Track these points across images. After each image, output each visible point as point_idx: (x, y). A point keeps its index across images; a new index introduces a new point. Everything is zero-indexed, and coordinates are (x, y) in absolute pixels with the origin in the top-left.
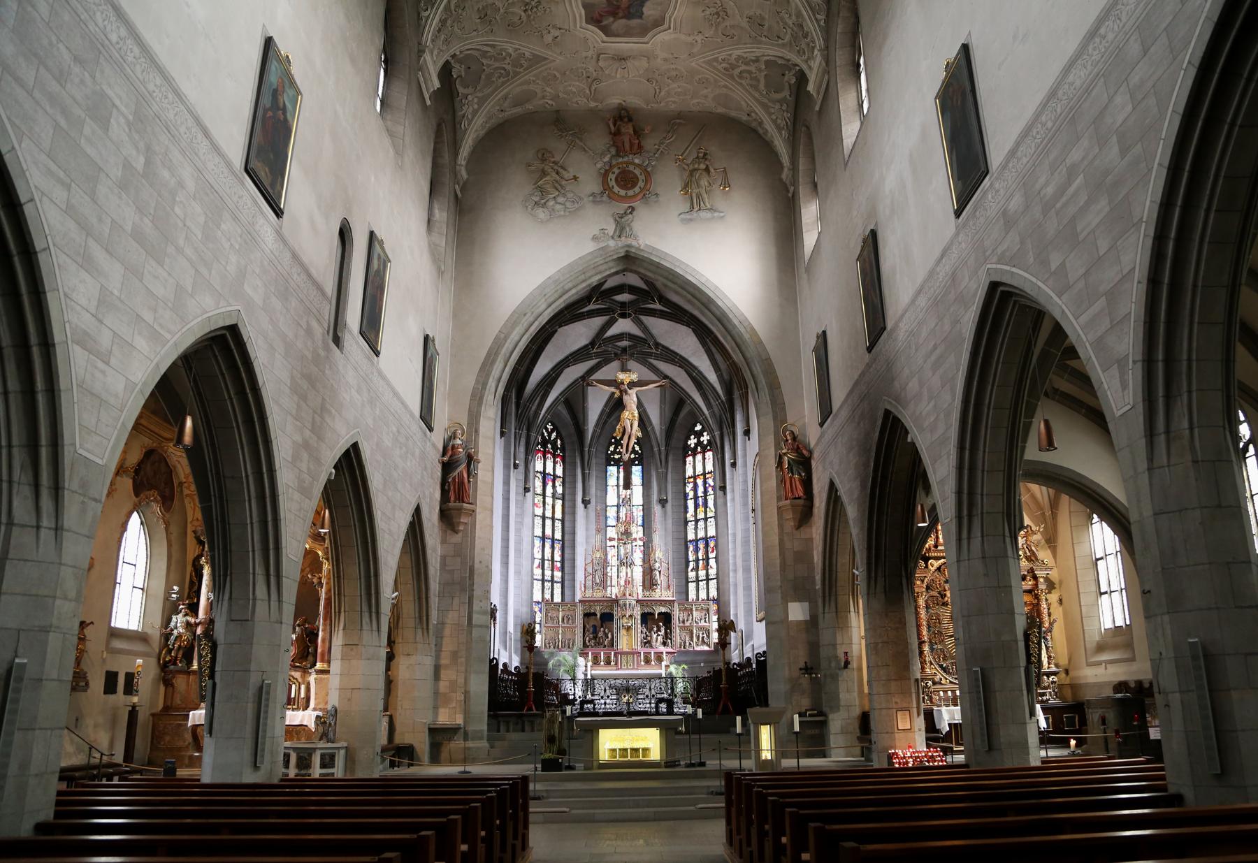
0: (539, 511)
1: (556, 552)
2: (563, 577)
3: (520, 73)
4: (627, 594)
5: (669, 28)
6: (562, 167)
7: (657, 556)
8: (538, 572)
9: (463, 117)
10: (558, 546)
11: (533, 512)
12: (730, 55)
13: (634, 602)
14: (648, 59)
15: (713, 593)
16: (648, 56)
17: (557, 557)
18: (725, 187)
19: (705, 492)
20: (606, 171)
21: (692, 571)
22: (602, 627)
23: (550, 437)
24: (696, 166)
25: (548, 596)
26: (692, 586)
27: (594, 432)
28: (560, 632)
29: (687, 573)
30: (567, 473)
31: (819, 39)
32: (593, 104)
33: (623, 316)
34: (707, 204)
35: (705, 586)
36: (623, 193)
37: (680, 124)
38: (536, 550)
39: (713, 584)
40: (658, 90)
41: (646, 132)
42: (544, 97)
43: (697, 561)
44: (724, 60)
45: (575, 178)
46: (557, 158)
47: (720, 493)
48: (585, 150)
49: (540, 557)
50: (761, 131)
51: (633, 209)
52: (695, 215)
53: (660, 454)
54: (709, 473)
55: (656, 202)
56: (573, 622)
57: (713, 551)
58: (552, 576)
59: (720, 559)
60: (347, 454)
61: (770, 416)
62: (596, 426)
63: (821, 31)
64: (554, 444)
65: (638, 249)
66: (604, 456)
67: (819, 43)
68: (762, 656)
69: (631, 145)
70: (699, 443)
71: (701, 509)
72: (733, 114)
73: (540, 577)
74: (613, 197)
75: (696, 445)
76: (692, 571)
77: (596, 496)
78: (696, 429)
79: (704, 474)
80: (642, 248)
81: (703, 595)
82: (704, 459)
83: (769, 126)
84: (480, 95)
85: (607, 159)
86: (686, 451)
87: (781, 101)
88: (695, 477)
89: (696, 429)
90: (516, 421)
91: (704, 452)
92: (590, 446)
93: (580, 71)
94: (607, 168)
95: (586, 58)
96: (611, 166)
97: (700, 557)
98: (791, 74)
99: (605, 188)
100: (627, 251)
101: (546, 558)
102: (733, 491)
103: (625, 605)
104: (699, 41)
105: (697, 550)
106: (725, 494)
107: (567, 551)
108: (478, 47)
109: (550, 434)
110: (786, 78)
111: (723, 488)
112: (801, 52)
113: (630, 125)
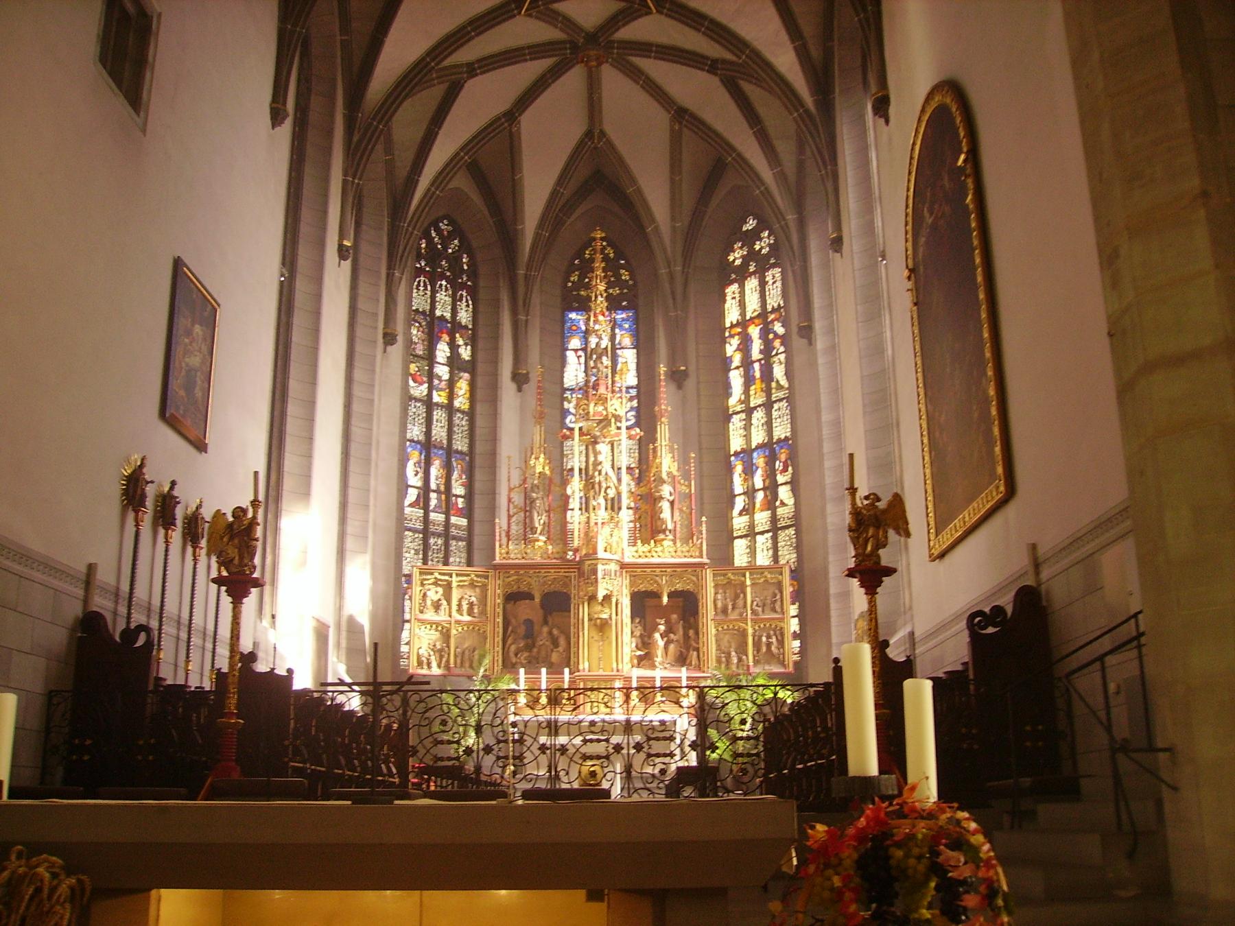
0: (420, 390)
1: (455, 475)
2: (470, 527)
7: (665, 469)
11: (406, 387)
15: (788, 556)
17: (458, 489)
19: (767, 351)
21: (740, 514)
22: (546, 622)
23: (445, 248)
26: (740, 546)
27: (537, 236)
30: (481, 321)
35: (769, 544)
38: (410, 468)
43: (750, 493)
47: (798, 343)
49: (419, 484)
53: (672, 277)
57: (785, 470)
59: (803, 481)
62: (541, 225)
64: (455, 260)
70: (752, 255)
73: (419, 526)
75: (746, 260)
76: (740, 514)
78: (744, 229)
79: (763, 315)
81: (763, 559)
82: (763, 284)
88: (743, 323)
89: (744, 229)
91: (761, 273)
92: (529, 267)
101: (433, 486)
102: (831, 331)
103: (595, 572)
105: (749, 471)
107: (479, 476)
109: (446, 242)
111: (807, 331)
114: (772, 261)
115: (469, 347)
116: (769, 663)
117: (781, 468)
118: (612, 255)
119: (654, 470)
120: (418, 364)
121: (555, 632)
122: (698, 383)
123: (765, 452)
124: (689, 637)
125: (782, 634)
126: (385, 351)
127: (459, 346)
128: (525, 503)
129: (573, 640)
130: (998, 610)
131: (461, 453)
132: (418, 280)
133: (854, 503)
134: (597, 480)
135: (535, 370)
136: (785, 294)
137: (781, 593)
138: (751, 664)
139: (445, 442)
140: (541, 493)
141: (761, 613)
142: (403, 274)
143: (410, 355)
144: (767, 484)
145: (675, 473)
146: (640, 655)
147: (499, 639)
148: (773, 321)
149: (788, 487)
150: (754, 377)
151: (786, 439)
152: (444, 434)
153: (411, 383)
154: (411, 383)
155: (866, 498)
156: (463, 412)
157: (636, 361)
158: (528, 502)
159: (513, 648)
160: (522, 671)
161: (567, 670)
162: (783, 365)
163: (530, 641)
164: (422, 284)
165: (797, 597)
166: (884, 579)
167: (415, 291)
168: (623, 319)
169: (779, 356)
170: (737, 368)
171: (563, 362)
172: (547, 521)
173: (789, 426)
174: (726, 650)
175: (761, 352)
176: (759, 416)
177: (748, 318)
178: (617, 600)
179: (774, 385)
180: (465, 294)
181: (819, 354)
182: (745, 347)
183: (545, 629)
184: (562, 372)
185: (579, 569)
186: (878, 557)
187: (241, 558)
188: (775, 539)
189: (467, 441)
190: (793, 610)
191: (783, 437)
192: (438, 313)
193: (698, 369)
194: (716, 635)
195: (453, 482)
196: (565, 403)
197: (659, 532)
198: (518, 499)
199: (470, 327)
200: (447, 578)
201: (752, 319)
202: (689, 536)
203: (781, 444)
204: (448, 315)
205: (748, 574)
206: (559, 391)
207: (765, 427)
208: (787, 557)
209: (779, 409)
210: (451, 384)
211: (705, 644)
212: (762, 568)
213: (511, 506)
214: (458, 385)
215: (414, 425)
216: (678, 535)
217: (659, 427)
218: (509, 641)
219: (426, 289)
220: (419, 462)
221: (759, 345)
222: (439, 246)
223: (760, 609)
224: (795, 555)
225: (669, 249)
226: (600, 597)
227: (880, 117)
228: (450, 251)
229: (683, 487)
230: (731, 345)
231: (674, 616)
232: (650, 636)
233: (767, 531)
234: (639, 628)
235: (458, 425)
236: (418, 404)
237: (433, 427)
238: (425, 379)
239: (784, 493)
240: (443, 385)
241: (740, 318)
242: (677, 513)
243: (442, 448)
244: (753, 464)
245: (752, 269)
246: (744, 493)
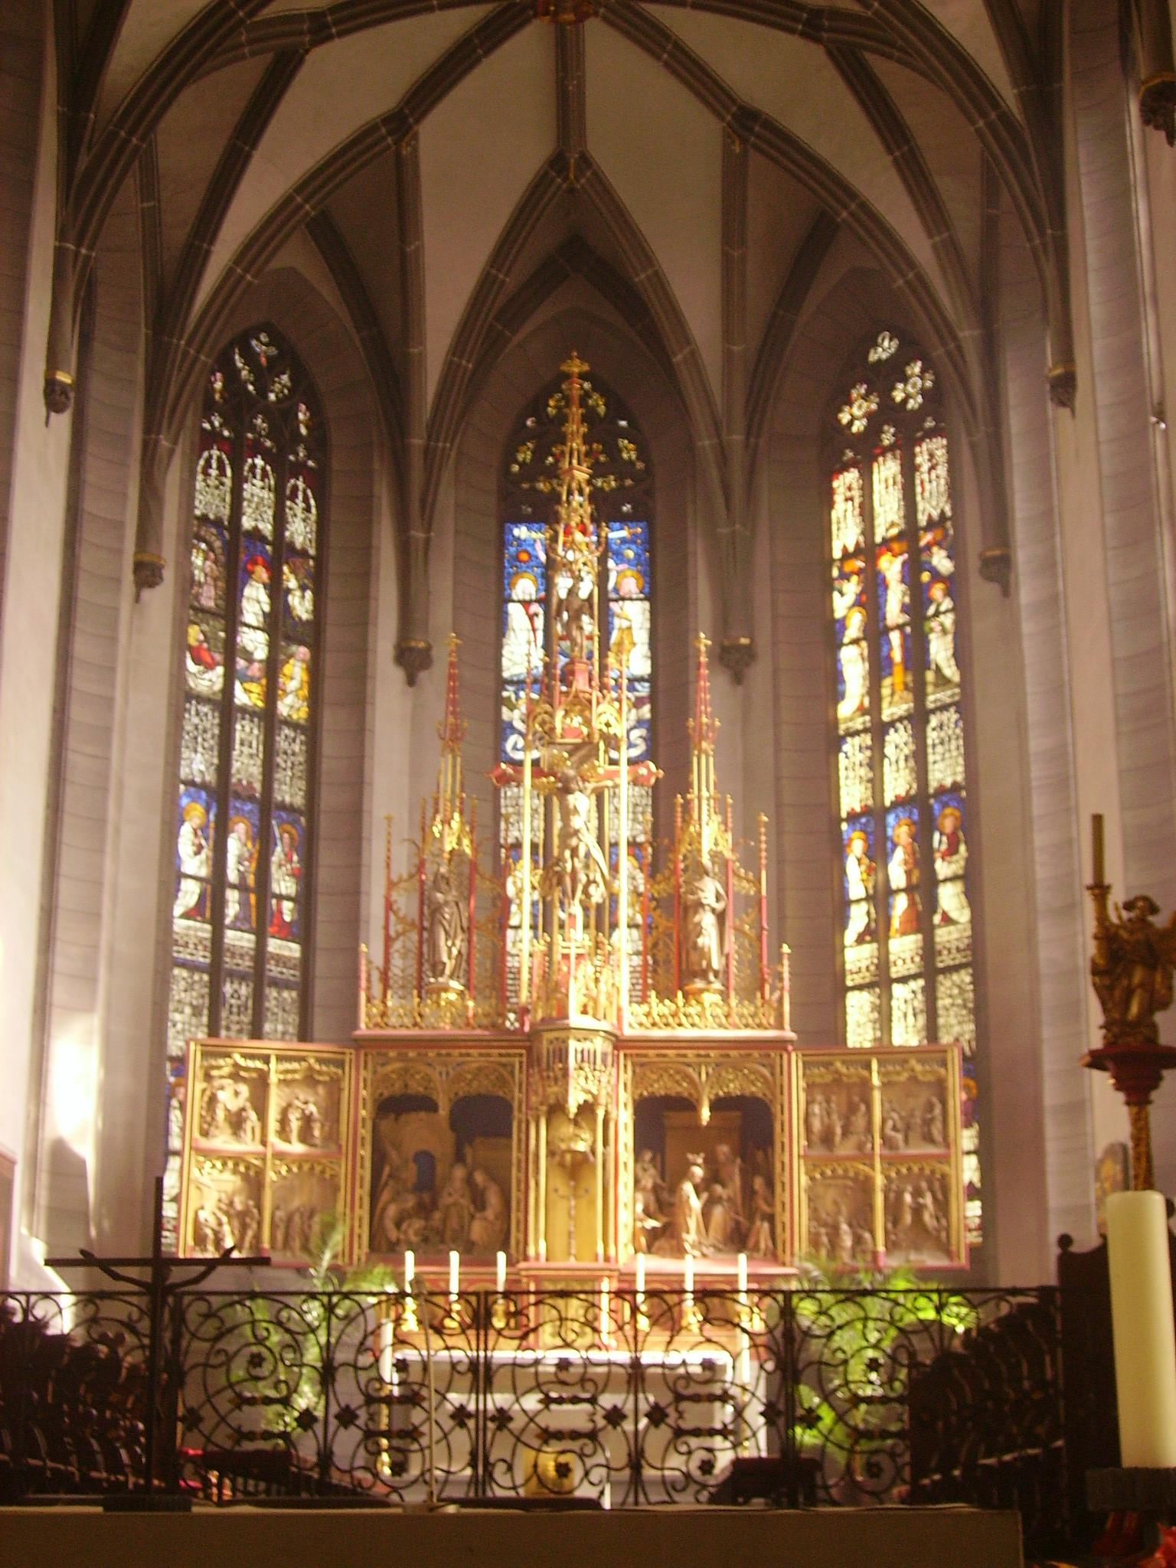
0: (208, 680)
1: (278, 855)
2: (306, 963)
7: (707, 845)
11: (179, 674)
15: (957, 1028)
17: (284, 884)
19: (917, 606)
21: (860, 940)
22: (459, 1157)
23: (263, 391)
26: (859, 1007)
27: (450, 371)
30: (335, 540)
35: (919, 1002)
43: (881, 897)
47: (982, 591)
49: (204, 872)
57: (952, 850)
59: (990, 873)
62: (458, 347)
64: (282, 417)
70: (888, 412)
73: (202, 957)
75: (875, 422)
76: (860, 940)
78: (873, 357)
79: (909, 533)
81: (906, 1033)
82: (909, 470)
88: (869, 551)
89: (873, 357)
101: (232, 876)
102: (1049, 566)
103: (562, 1055)
105: (878, 852)
106: (1007, 590)
107: (327, 857)
109: (264, 377)
115: (309, 594)
116: (917, 1248)
117: (944, 847)
118: (602, 410)
119: (684, 849)
120: (205, 627)
121: (479, 1178)
122: (775, 671)
123: (911, 813)
124: (753, 1193)
125: (945, 1189)
126: (137, 599)
127: (288, 591)
128: (422, 913)
129: (514, 1194)
131: (290, 809)
132: (206, 454)
133: (1102, 917)
134: (569, 866)
135: (445, 644)
136: (954, 491)
137: (944, 1103)
138: (881, 1248)
139: (258, 786)
140: (454, 893)
141: (901, 1143)
142: (175, 442)
143: (189, 609)
144: (914, 880)
145: (728, 854)
146: (654, 1228)
147: (363, 1192)
148: (929, 547)
150: (889, 660)
151: (956, 787)
152: (256, 771)
153: (191, 665)
154: (191, 665)
155: (1129, 906)
156: (295, 726)
157: (648, 625)
158: (426, 911)
159: (392, 1211)
160: (410, 1256)
161: (501, 1257)
162: (950, 637)
163: (426, 1197)
164: (214, 464)
165: (977, 1112)
166: (1166, 1073)
167: (200, 477)
168: (623, 541)
169: (942, 618)
170: (855, 642)
171: (501, 626)
172: (464, 951)
173: (961, 761)
174: (830, 1220)
175: (905, 609)
176: (898, 741)
177: (878, 539)
178: (607, 1113)
179: (930, 676)
180: (301, 484)
181: (1024, 614)
182: (872, 598)
183: (459, 1173)
184: (499, 647)
185: (529, 1050)
186: (1154, 1028)
188: (930, 994)
189: (302, 784)
190: (968, 1138)
191: (948, 782)
192: (247, 523)
193: (774, 644)
194: (810, 1190)
195: (274, 868)
196: (504, 710)
198: (406, 903)
199: (312, 552)
200: (259, 1064)
201: (886, 541)
202: (755, 986)
203: (945, 799)
204: (267, 528)
205: (875, 1065)
206: (491, 684)
207: (912, 763)
208: (956, 1029)
209: (941, 727)
210: (272, 668)
211: (787, 1206)
212: (906, 1052)
213: (392, 917)
214: (287, 669)
215: (196, 751)
216: (732, 982)
217: (695, 760)
218: (385, 1196)
219: (222, 472)
220: (204, 828)
221: (899, 595)
222: (251, 388)
223: (899, 1137)
224: (972, 1027)
226: (573, 1109)
227: (1157, 128)
228: (272, 397)
229: (745, 884)
230: (842, 594)
231: (724, 1149)
232: (674, 1188)
233: (915, 977)
234: (652, 1171)
235: (285, 753)
236: (205, 709)
237: (235, 753)
238: (218, 657)
239: (950, 898)
240: (256, 669)
241: (861, 539)
242: (730, 937)
243: (251, 798)
244: (885, 838)
245: (887, 439)
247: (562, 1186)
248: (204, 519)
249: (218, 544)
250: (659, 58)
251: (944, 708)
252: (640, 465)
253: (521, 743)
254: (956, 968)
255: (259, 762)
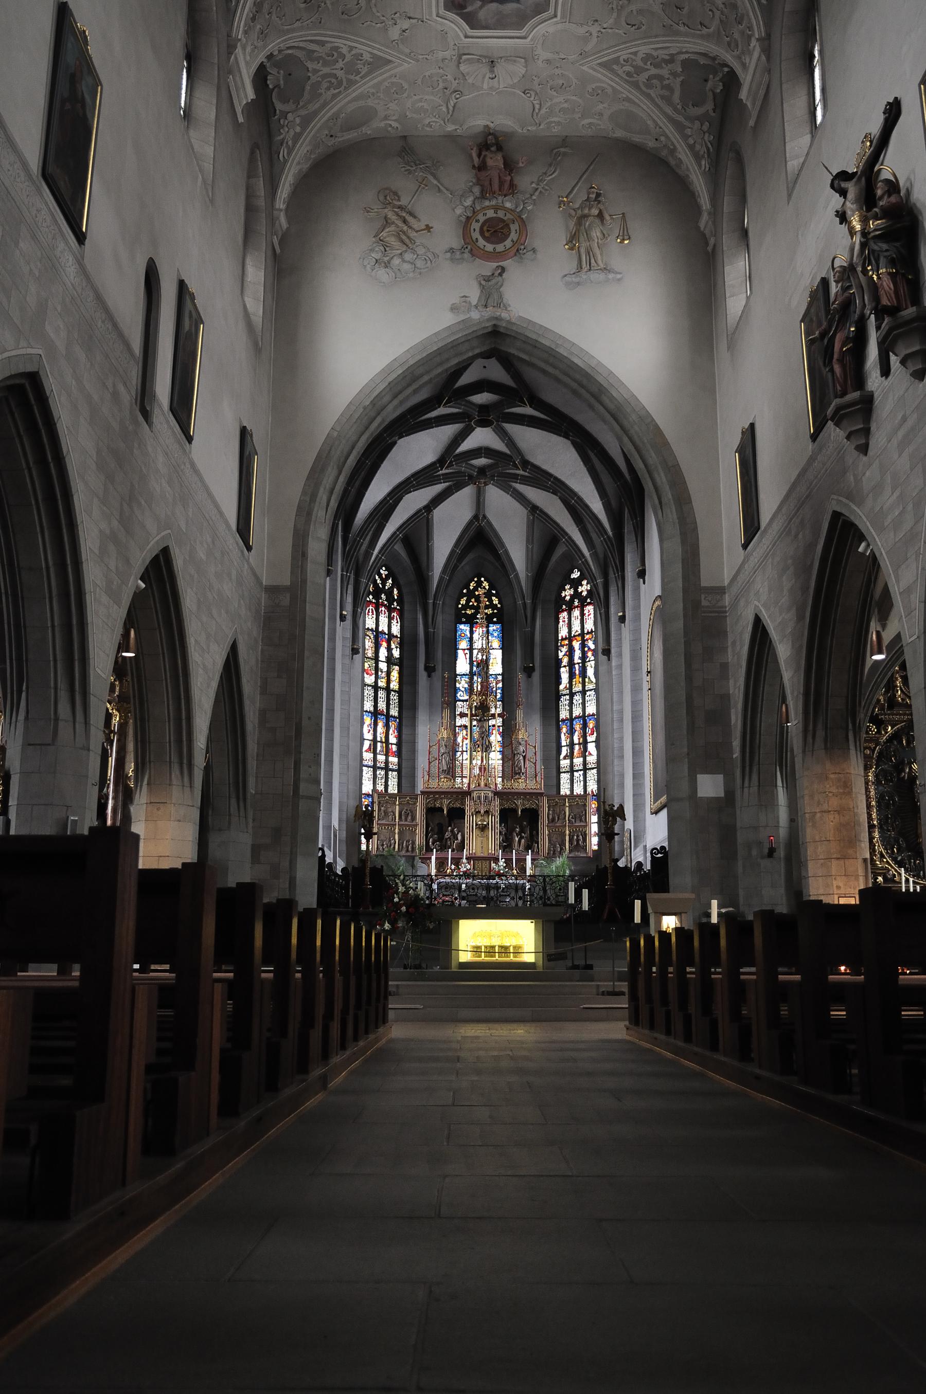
0: (370, 679)
1: (391, 732)
2: (400, 764)
3: (356, 82)
4: (482, 784)
5: (555, 16)
6: (411, 214)
8: (368, 756)
9: (282, 145)
10: (393, 726)
11: (363, 678)
12: (635, 54)
13: (490, 795)
14: (526, 61)
15: (592, 787)
16: (527, 57)
17: (393, 739)
18: (623, 240)
19: (584, 658)
20: (468, 218)
21: (565, 758)
22: (450, 825)
24: (586, 211)
25: (381, 788)
26: (564, 778)
27: (441, 579)
28: (397, 831)
29: (558, 761)
31: (759, 28)
32: (450, 128)
33: (484, 423)
34: (600, 262)
35: (582, 778)
36: (490, 247)
37: (565, 154)
39: (592, 775)
40: (537, 106)
41: (521, 165)
42: (386, 118)
43: (571, 745)
44: (626, 61)
45: (428, 228)
46: (404, 202)
47: (602, 658)
48: (439, 190)
49: (371, 737)
50: (672, 162)
51: (503, 269)
52: (584, 277)
54: (588, 633)
55: (532, 260)
56: (414, 819)
58: (387, 762)
60: (155, 561)
61: (678, 540)
63: (761, 12)
64: (389, 594)
65: (509, 322)
66: (453, 612)
67: (758, 30)
68: (659, 852)
69: (501, 183)
70: (577, 595)
71: (578, 680)
72: (637, 139)
73: (371, 763)
74: (475, 253)
76: (565, 758)
77: (443, 661)
79: (582, 634)
80: (513, 320)
81: (578, 790)
83: (684, 155)
84: (303, 112)
85: (468, 202)
86: (559, 605)
87: (701, 119)
90: (343, 561)
91: (582, 607)
93: (435, 79)
94: (470, 215)
95: (443, 60)
96: (474, 212)
97: (576, 740)
98: (718, 78)
99: (467, 241)
100: (495, 325)
101: (379, 739)
103: (479, 798)
104: (595, 34)
105: (571, 732)
108: (301, 44)
109: (384, 582)
110: (710, 84)
111: (607, 652)
112: (733, 45)
113: (499, 157)
114: (589, 600)
115: (398, 649)
117: (590, 732)
120: (369, 663)
126: (352, 659)
127: (392, 649)
130: (663, 848)
131: (394, 717)
139: (385, 711)
148: (587, 640)
149: (594, 744)
151: (593, 715)
152: (384, 706)
153: (365, 675)
154: (365, 675)
156: (395, 691)
164: (370, 611)
167: (367, 616)
173: (595, 706)
175: (580, 658)
179: (587, 680)
180: (395, 615)
187: (370, 825)
189: (397, 709)
192: (380, 630)
194: (549, 835)
196: (457, 684)
197: (517, 773)
199: (399, 636)
201: (574, 636)
203: (590, 717)
204: (386, 631)
206: (453, 676)
210: (388, 674)
214: (392, 674)
219: (373, 614)
223: (573, 820)
224: (596, 786)
225: (524, 588)
226: (482, 812)
228: (387, 588)
230: (561, 652)
232: (511, 834)
233: (581, 770)
238: (373, 672)
239: (592, 747)
240: (384, 675)
241: (567, 635)
243: (383, 715)
245: (576, 603)
246: (567, 746)
247: (479, 832)
248: (368, 629)
249: (372, 637)
250: (508, 494)
251: (590, 690)
252: (499, 606)
253: (462, 694)
254: (593, 768)
255: (385, 703)
